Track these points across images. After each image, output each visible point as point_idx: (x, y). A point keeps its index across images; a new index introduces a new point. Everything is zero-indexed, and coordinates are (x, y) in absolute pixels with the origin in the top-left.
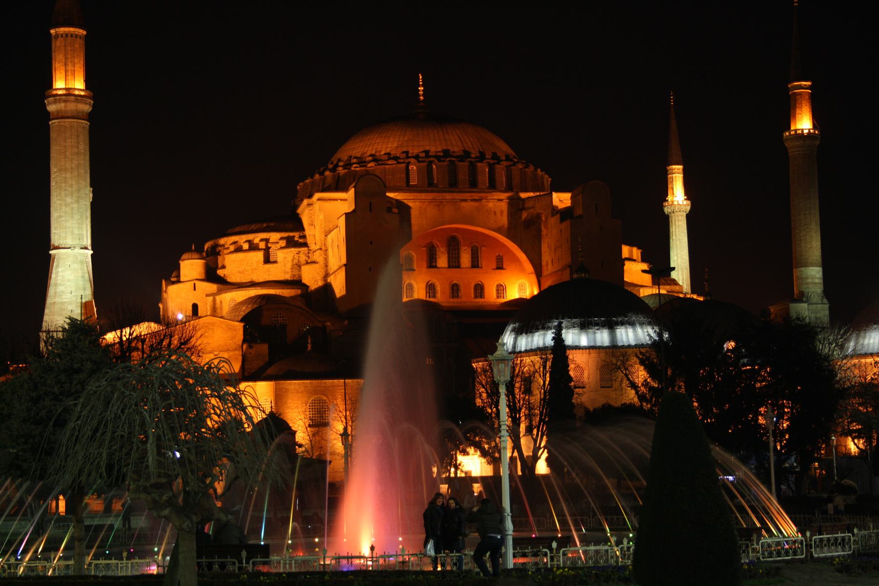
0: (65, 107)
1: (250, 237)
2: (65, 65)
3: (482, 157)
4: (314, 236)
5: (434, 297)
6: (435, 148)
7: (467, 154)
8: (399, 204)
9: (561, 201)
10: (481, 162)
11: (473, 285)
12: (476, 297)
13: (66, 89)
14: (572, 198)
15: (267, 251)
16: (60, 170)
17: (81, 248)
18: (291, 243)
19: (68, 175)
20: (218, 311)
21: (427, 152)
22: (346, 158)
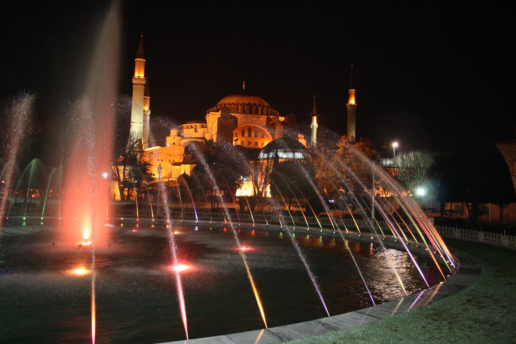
0: (138, 82)
1: (191, 124)
2: (139, 69)
3: (260, 105)
4: (209, 125)
5: (243, 145)
6: (246, 102)
7: (255, 104)
8: (235, 117)
9: (281, 119)
10: (259, 107)
11: (255, 142)
12: (255, 145)
13: (138, 76)
14: (285, 118)
15: (196, 129)
16: (135, 100)
17: (140, 123)
18: (203, 127)
19: (137, 101)
20: (180, 145)
21: (244, 103)
22: (220, 104)
